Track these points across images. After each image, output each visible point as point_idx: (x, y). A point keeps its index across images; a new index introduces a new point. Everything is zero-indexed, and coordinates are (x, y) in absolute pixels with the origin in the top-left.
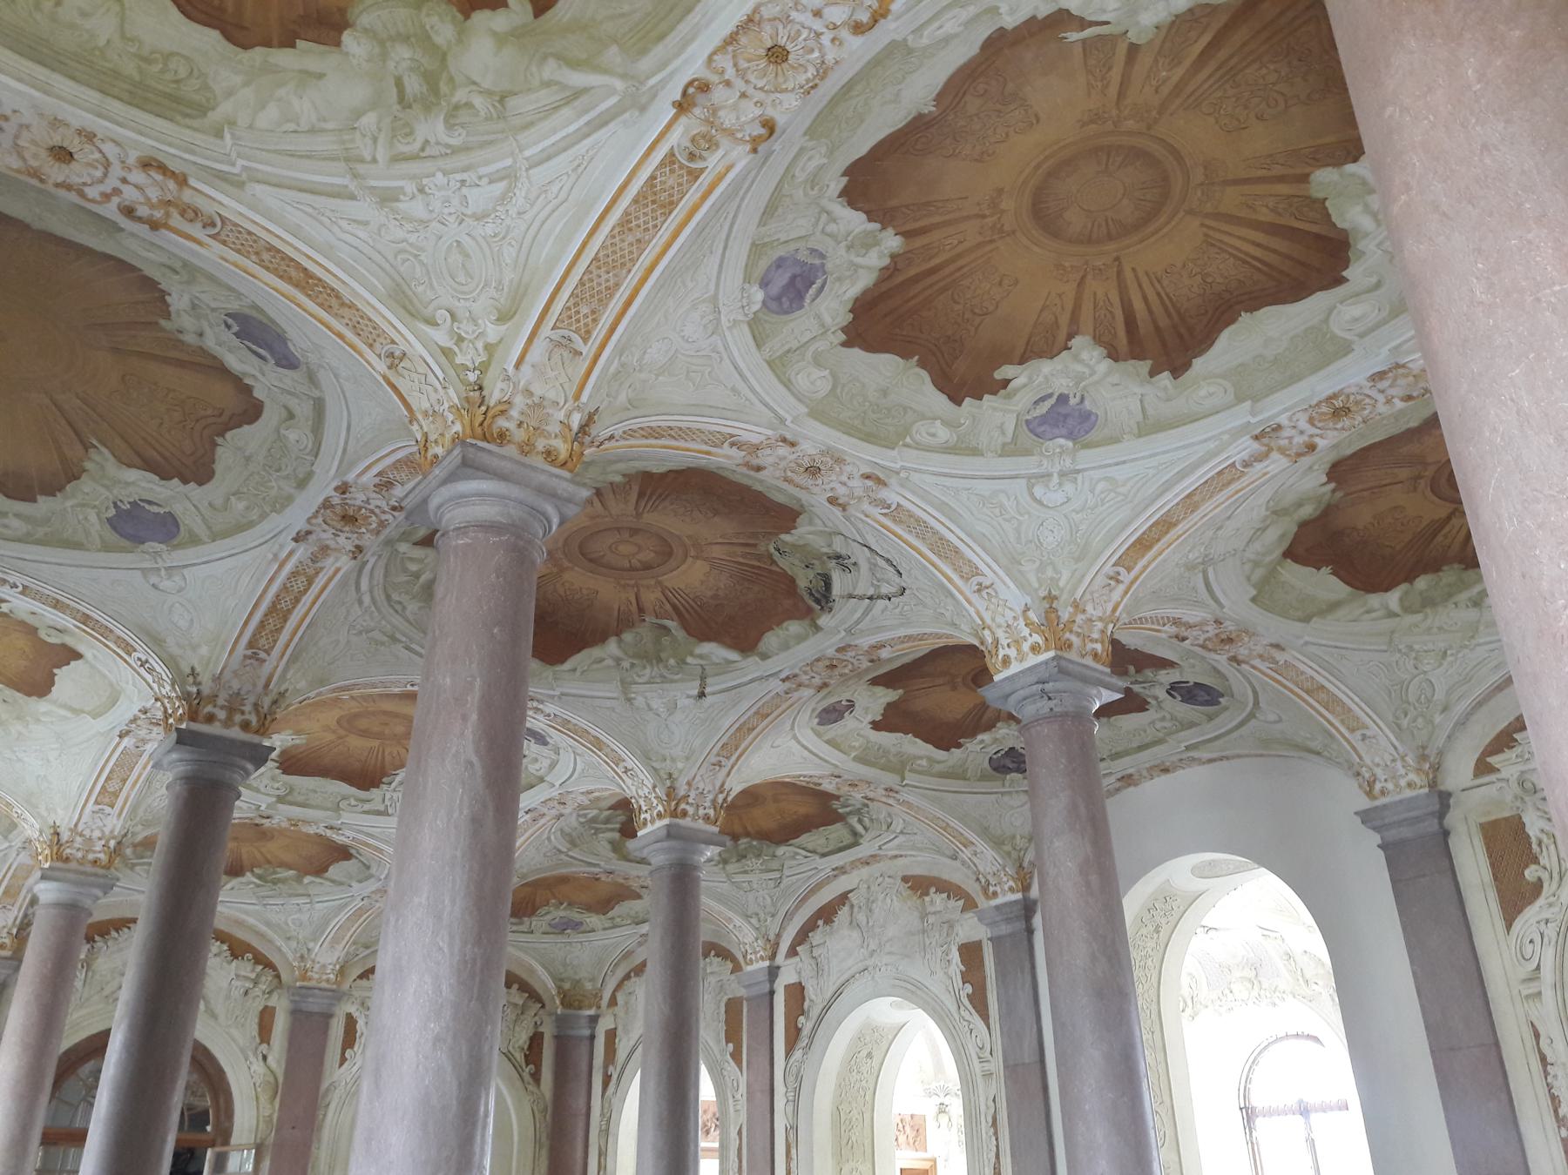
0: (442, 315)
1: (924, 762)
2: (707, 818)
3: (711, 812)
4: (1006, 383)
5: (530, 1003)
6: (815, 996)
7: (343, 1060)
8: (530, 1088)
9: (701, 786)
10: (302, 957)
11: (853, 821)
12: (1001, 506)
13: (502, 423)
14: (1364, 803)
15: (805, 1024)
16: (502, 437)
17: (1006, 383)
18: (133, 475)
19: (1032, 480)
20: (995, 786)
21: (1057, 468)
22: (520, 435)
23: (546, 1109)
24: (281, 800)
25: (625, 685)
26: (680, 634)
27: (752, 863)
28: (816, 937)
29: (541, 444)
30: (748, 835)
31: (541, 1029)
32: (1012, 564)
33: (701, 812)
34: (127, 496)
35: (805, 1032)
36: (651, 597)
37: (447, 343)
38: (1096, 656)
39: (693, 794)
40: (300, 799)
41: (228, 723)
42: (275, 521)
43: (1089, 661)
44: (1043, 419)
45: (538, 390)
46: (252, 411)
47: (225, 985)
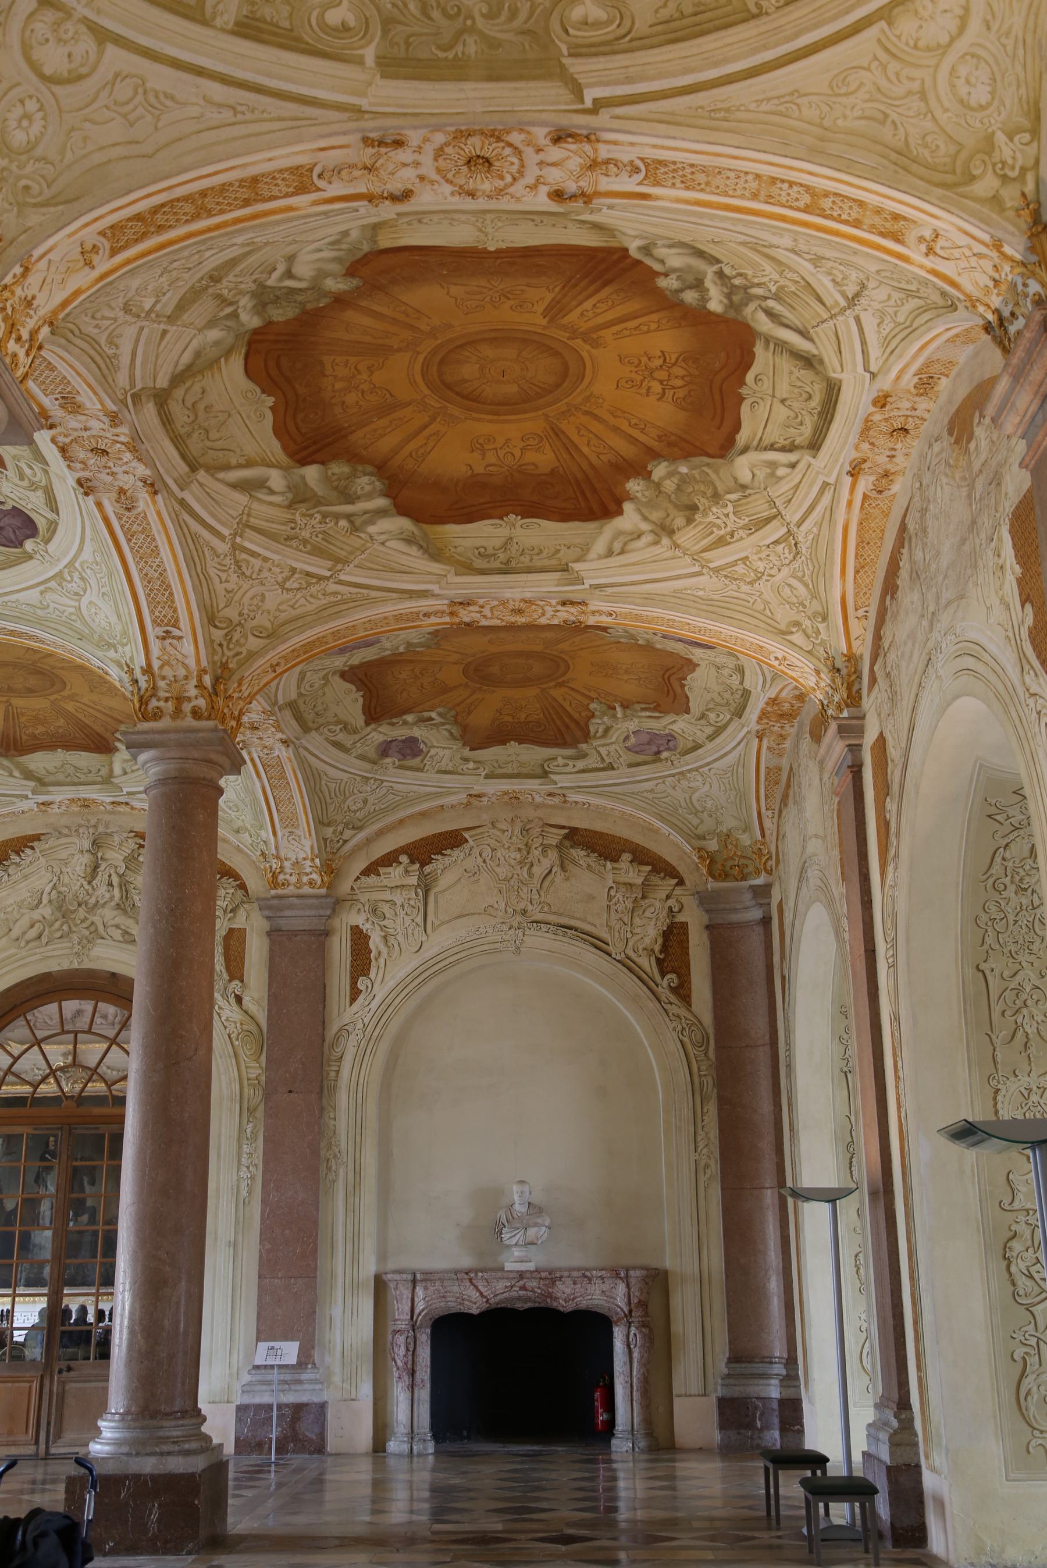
5: (655, 880)
7: (355, 994)
8: (673, 1009)
10: (263, 854)
23: (704, 1041)
27: (720, 517)
30: (655, 455)
31: (681, 918)
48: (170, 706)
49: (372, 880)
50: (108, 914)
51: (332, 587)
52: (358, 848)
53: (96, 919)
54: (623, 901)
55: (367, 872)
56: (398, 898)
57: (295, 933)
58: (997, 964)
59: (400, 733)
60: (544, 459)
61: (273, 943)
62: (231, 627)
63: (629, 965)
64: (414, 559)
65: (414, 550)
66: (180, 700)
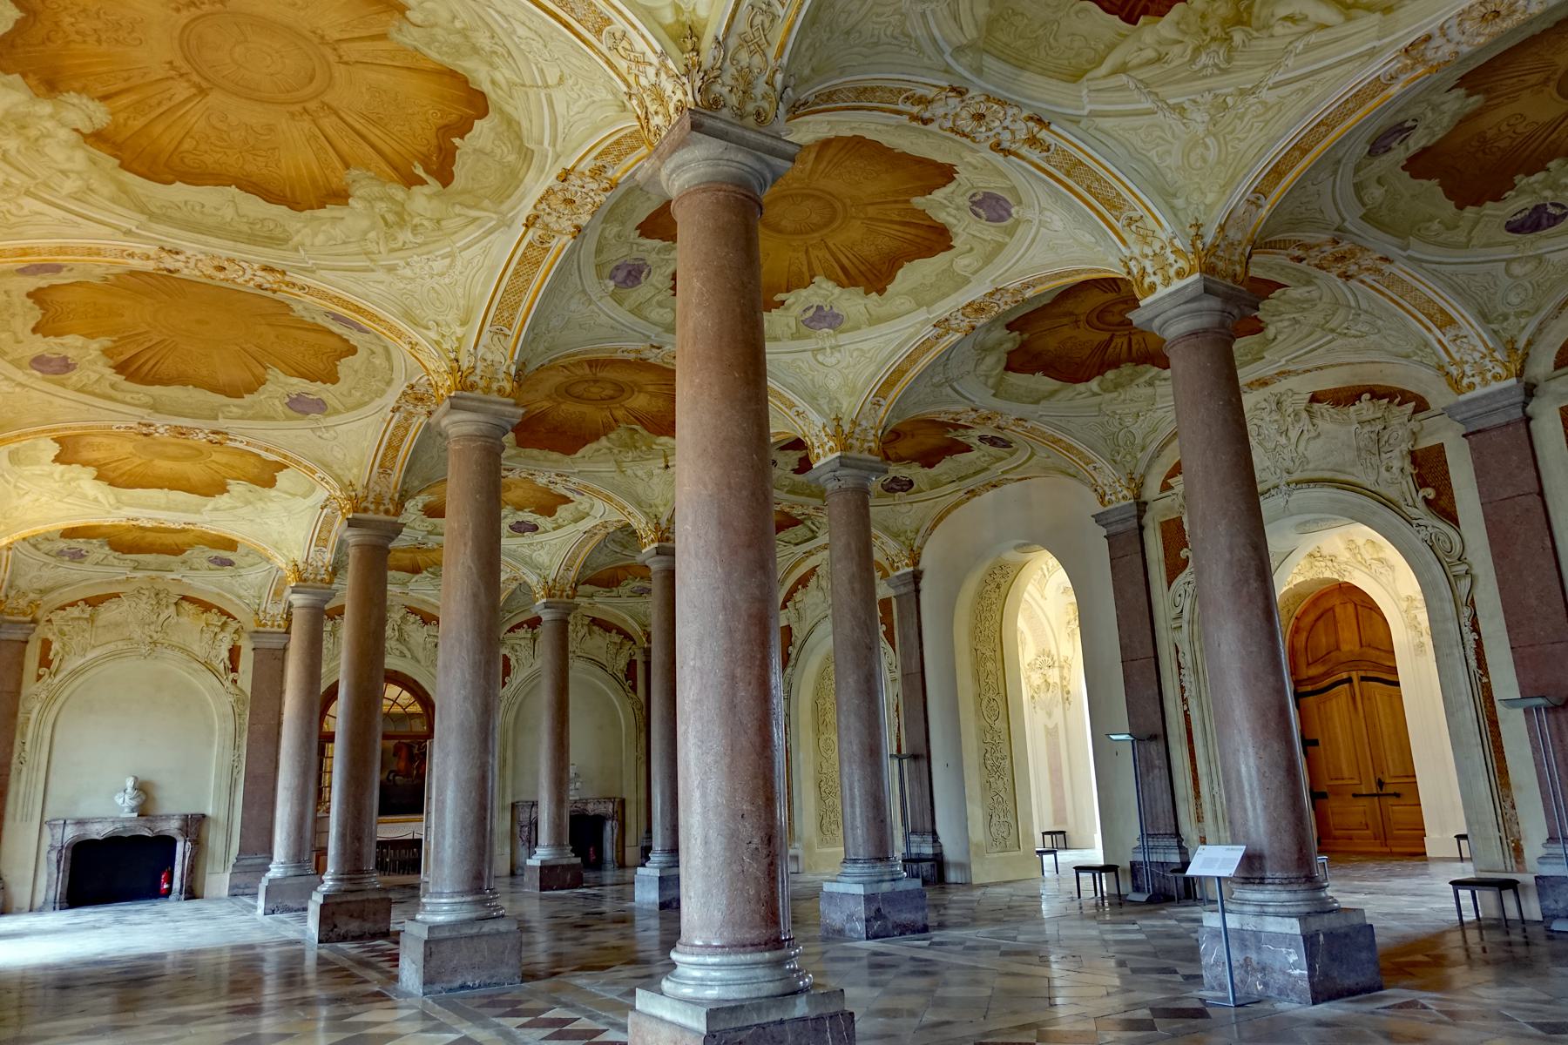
0: (431, 324)
4: (783, 303)
6: (798, 634)
7: (504, 684)
11: (809, 523)
13: (472, 378)
14: (1100, 509)
15: (793, 651)
16: (473, 387)
17: (783, 303)
18: (295, 380)
19: (815, 352)
20: (889, 501)
21: (827, 344)
22: (482, 383)
24: (430, 533)
26: (645, 433)
28: (798, 596)
29: (495, 386)
32: (812, 399)
34: (294, 391)
35: (793, 656)
36: (619, 413)
37: (436, 337)
38: (870, 450)
41: (377, 511)
42: (378, 402)
43: (866, 455)
44: (812, 319)
45: (489, 357)
46: (353, 351)
47: (421, 641)
54: (613, 650)
56: (523, 643)
58: (821, 701)
63: (614, 676)
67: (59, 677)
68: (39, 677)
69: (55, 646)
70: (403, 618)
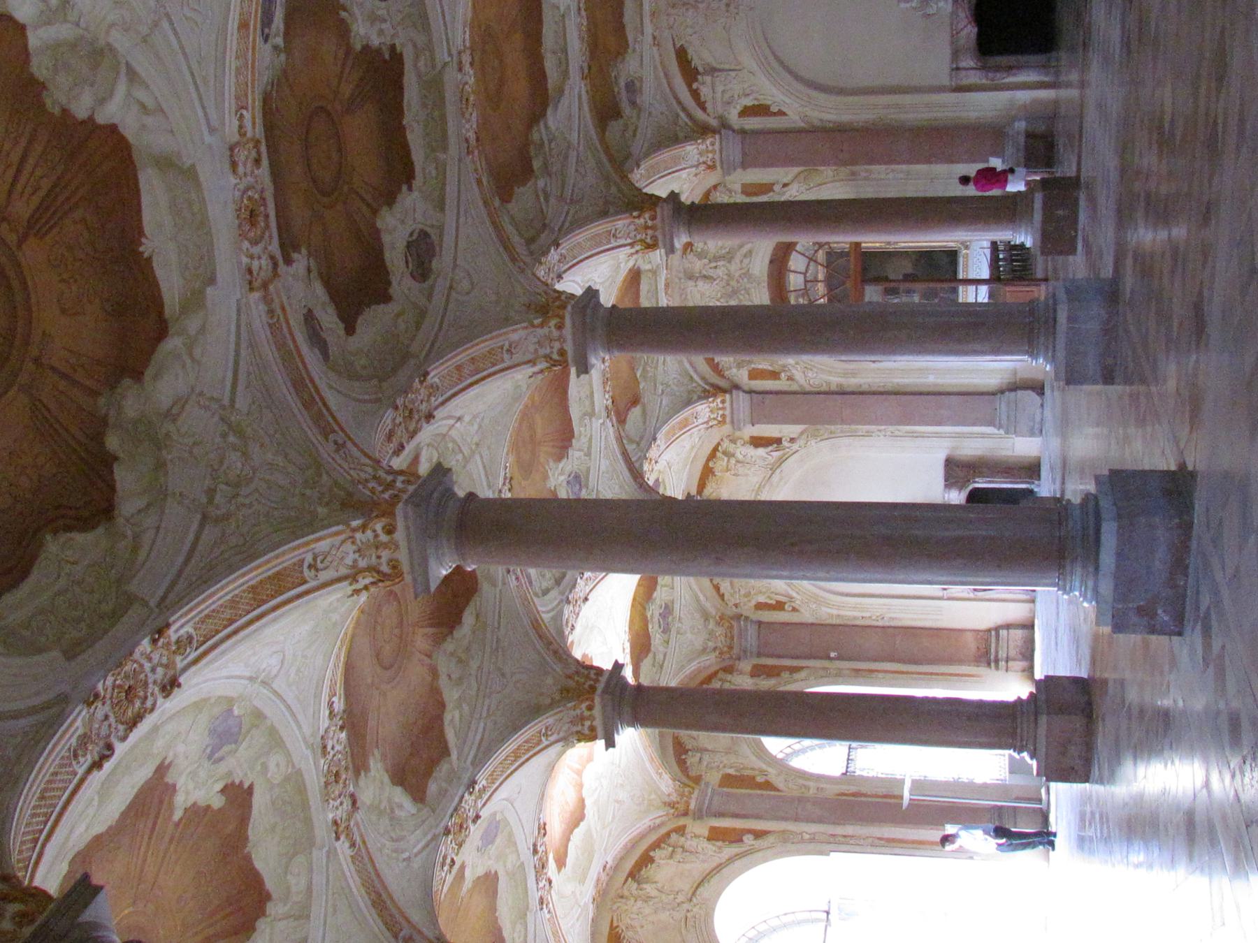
1: (421, 64)
2: (560, 327)
3: (553, 322)
7: (781, 113)
9: (532, 348)
10: (696, 175)
12: (298, 670)
25: (466, 460)
33: (556, 333)
39: (542, 352)
40: (587, 403)
41: (592, 718)
43: (400, 535)
48: (650, 232)
49: (709, 106)
50: (734, 267)
51: (581, 148)
52: (689, 115)
53: (737, 275)
55: (704, 109)
56: (720, 88)
57: (744, 154)
59: (623, 92)
60: (518, 37)
61: (750, 166)
62: (606, 203)
64: (565, 102)
65: (560, 106)
66: (647, 227)
67: (794, 595)
68: (794, 610)
69: (762, 599)
70: (701, 256)
